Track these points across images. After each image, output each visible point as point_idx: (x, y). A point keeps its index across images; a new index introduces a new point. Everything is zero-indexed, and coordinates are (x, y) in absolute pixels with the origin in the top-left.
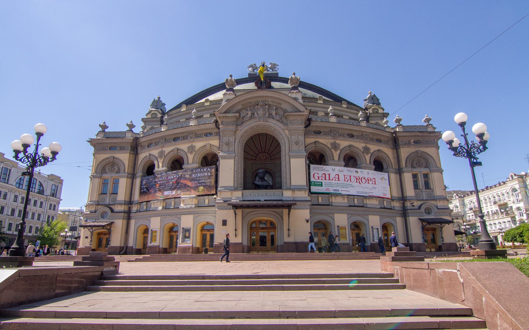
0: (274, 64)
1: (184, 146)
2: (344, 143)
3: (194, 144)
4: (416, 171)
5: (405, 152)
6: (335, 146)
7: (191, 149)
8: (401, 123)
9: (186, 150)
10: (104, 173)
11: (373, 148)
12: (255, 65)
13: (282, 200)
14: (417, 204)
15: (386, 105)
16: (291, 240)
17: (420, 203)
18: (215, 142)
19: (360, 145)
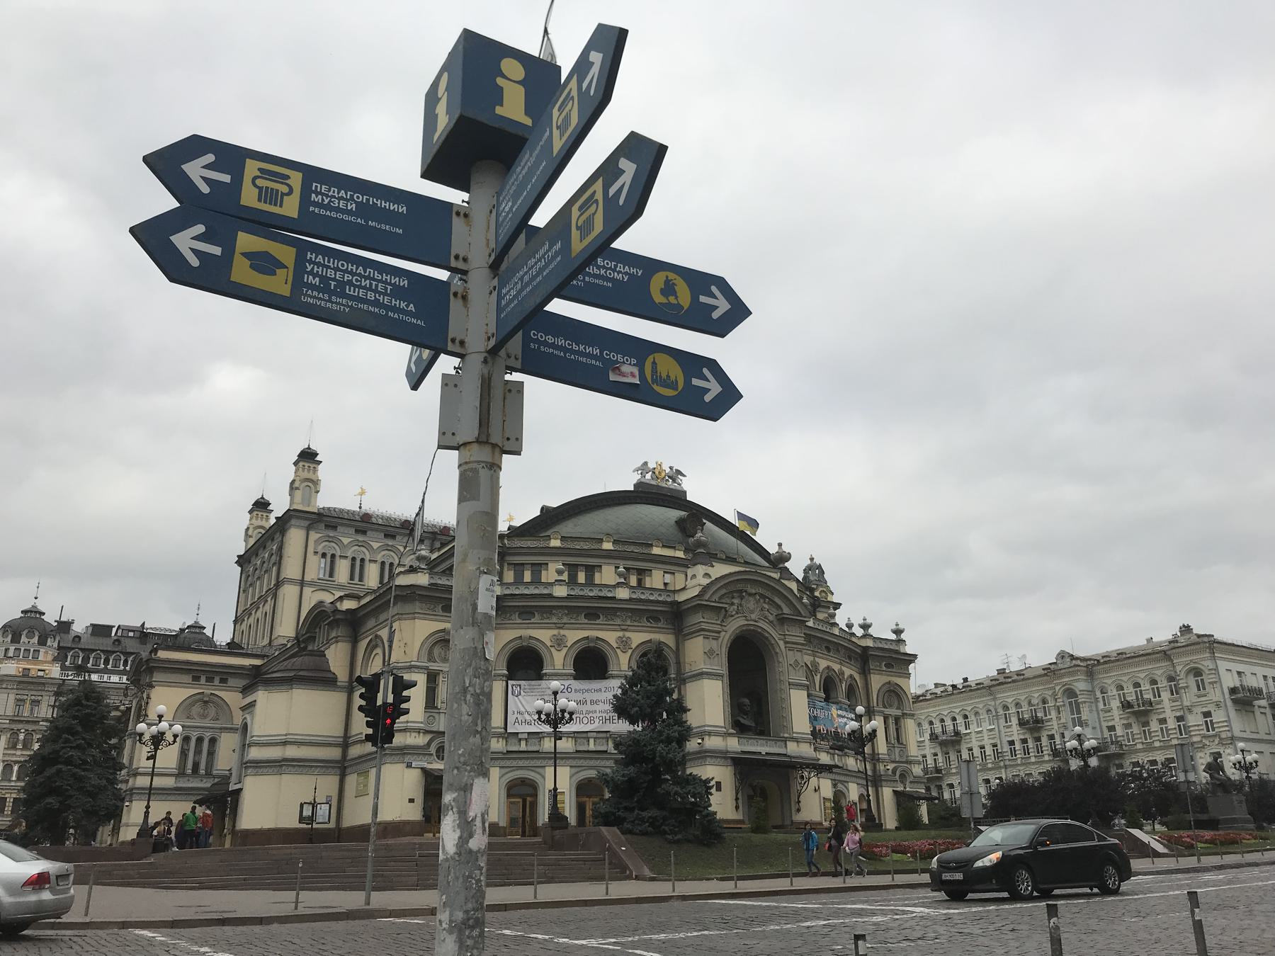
0: (679, 472)
1: (611, 637)
2: (823, 664)
3: (628, 634)
4: (888, 711)
5: (877, 681)
6: (816, 665)
7: (624, 643)
8: (871, 631)
9: (615, 645)
10: (429, 660)
11: (848, 672)
12: (646, 463)
13: (785, 755)
14: (891, 767)
15: (839, 586)
16: (799, 818)
17: (894, 765)
18: (668, 639)
19: (836, 667)
